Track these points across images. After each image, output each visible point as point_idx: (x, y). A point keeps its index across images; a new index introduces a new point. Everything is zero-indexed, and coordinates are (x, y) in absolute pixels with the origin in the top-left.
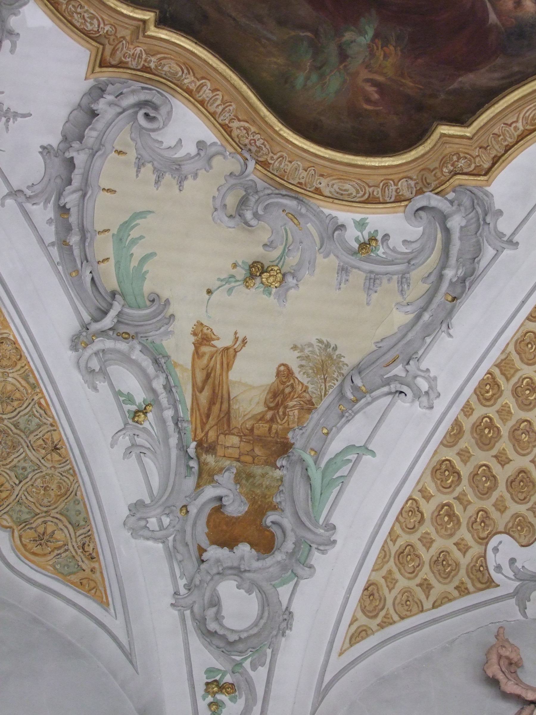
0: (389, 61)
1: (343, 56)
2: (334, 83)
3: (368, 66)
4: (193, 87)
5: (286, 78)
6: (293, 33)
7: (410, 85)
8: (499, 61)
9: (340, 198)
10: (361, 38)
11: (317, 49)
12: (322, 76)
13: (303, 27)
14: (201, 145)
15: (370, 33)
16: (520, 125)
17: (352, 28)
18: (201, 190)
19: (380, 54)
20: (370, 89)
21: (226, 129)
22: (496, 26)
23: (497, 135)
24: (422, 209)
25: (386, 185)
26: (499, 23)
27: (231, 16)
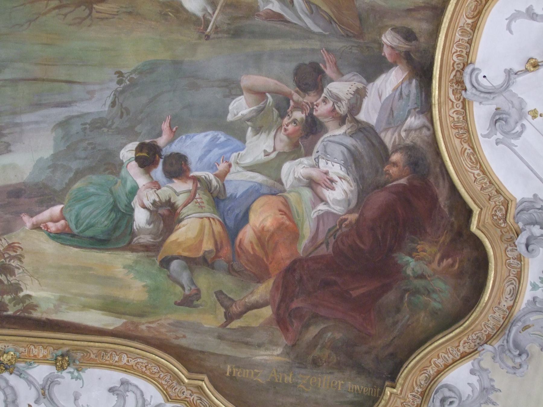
0: (427, 248)
1: (422, 277)
2: (439, 285)
3: (430, 263)
4: (436, 369)
5: (434, 313)
6: (406, 305)
7: (445, 238)
8: (432, 180)
9: (516, 294)
10: (411, 265)
11: (416, 292)
12: (434, 291)
13: (402, 298)
14: (472, 372)
15: (408, 258)
16: (476, 172)
17: (404, 269)
18: (501, 379)
19: (422, 254)
20: (445, 263)
21: (464, 356)
22: (408, 179)
23: (482, 189)
24: (527, 246)
25: (510, 265)
26: (406, 178)
27: (392, 340)
